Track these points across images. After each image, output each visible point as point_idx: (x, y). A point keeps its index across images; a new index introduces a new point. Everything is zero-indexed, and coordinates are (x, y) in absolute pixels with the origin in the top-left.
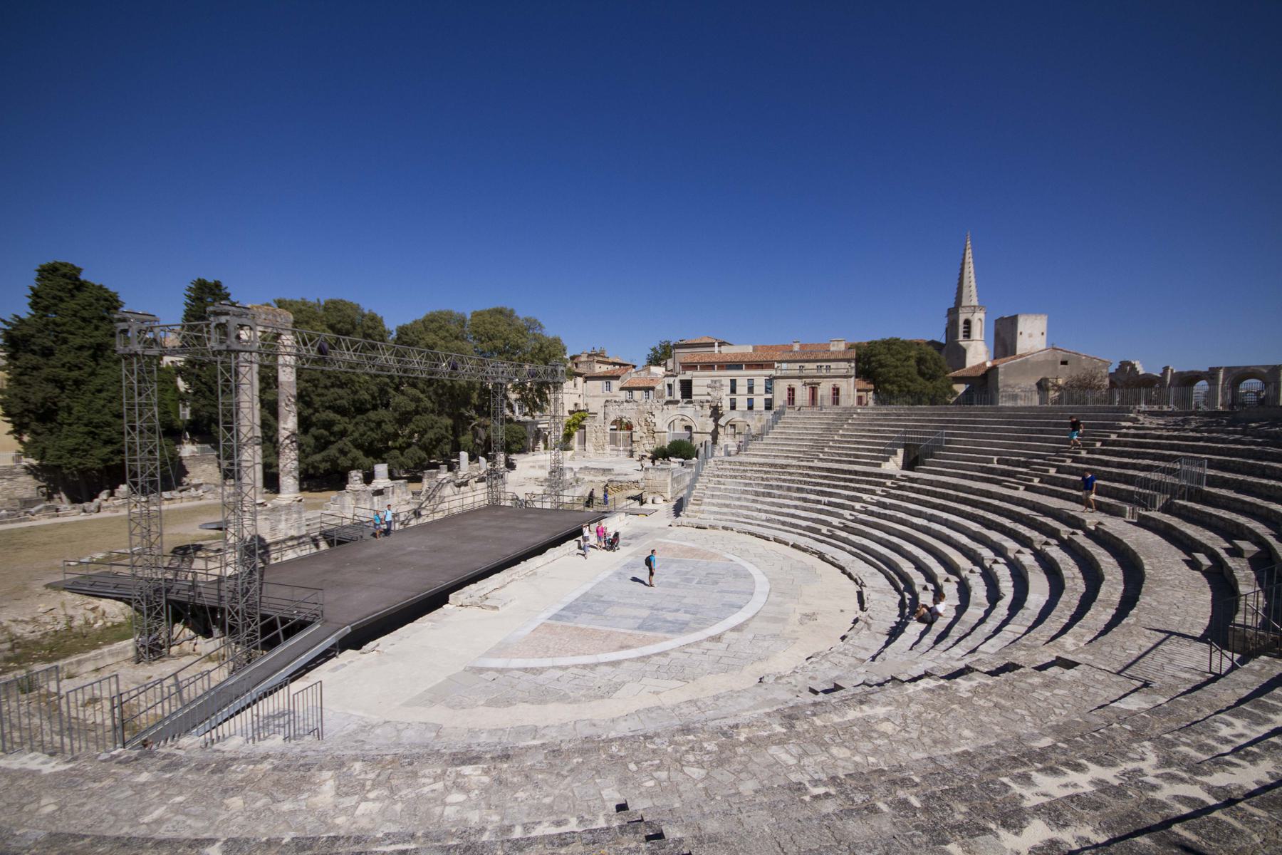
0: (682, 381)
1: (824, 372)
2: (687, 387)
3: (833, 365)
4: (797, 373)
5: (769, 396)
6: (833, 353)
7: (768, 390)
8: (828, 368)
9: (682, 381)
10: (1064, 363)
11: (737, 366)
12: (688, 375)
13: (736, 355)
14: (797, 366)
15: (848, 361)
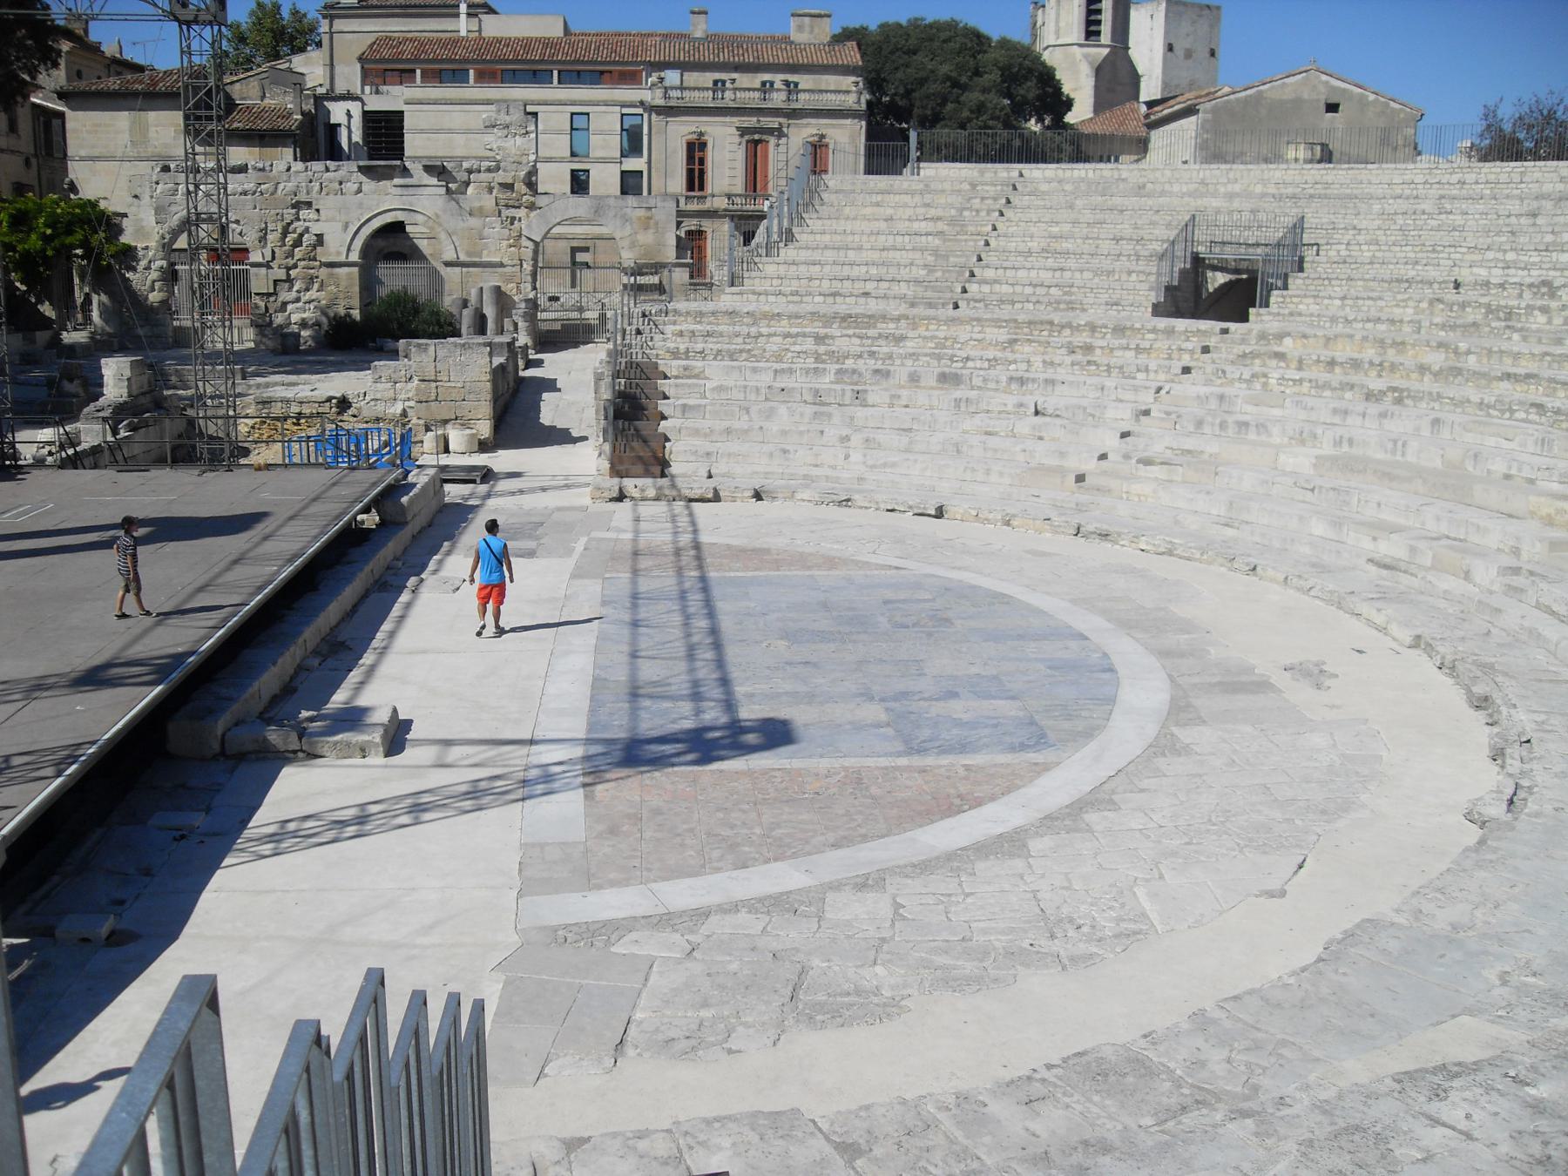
0: (370, 118)
1: (778, 99)
2: (385, 135)
3: (805, 81)
4: (705, 99)
5: (633, 164)
6: (801, 48)
7: (633, 142)
8: (792, 88)
9: (370, 118)
10: (1332, 108)
11: (537, 76)
12: (390, 98)
13: (527, 43)
14: (707, 78)
15: (846, 70)
